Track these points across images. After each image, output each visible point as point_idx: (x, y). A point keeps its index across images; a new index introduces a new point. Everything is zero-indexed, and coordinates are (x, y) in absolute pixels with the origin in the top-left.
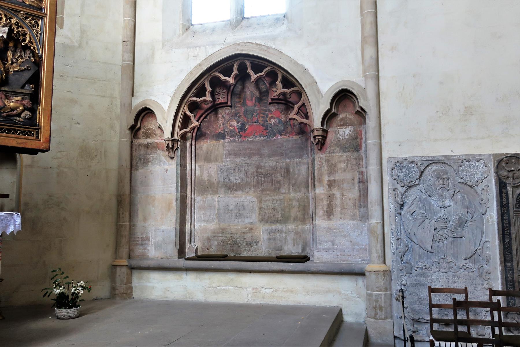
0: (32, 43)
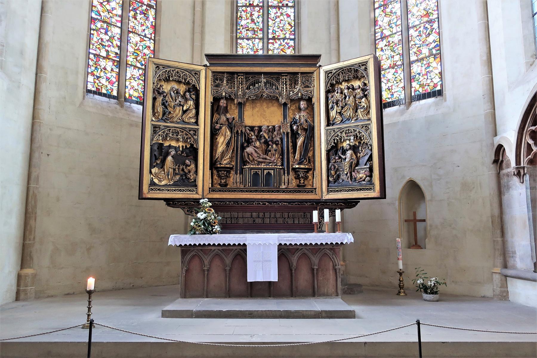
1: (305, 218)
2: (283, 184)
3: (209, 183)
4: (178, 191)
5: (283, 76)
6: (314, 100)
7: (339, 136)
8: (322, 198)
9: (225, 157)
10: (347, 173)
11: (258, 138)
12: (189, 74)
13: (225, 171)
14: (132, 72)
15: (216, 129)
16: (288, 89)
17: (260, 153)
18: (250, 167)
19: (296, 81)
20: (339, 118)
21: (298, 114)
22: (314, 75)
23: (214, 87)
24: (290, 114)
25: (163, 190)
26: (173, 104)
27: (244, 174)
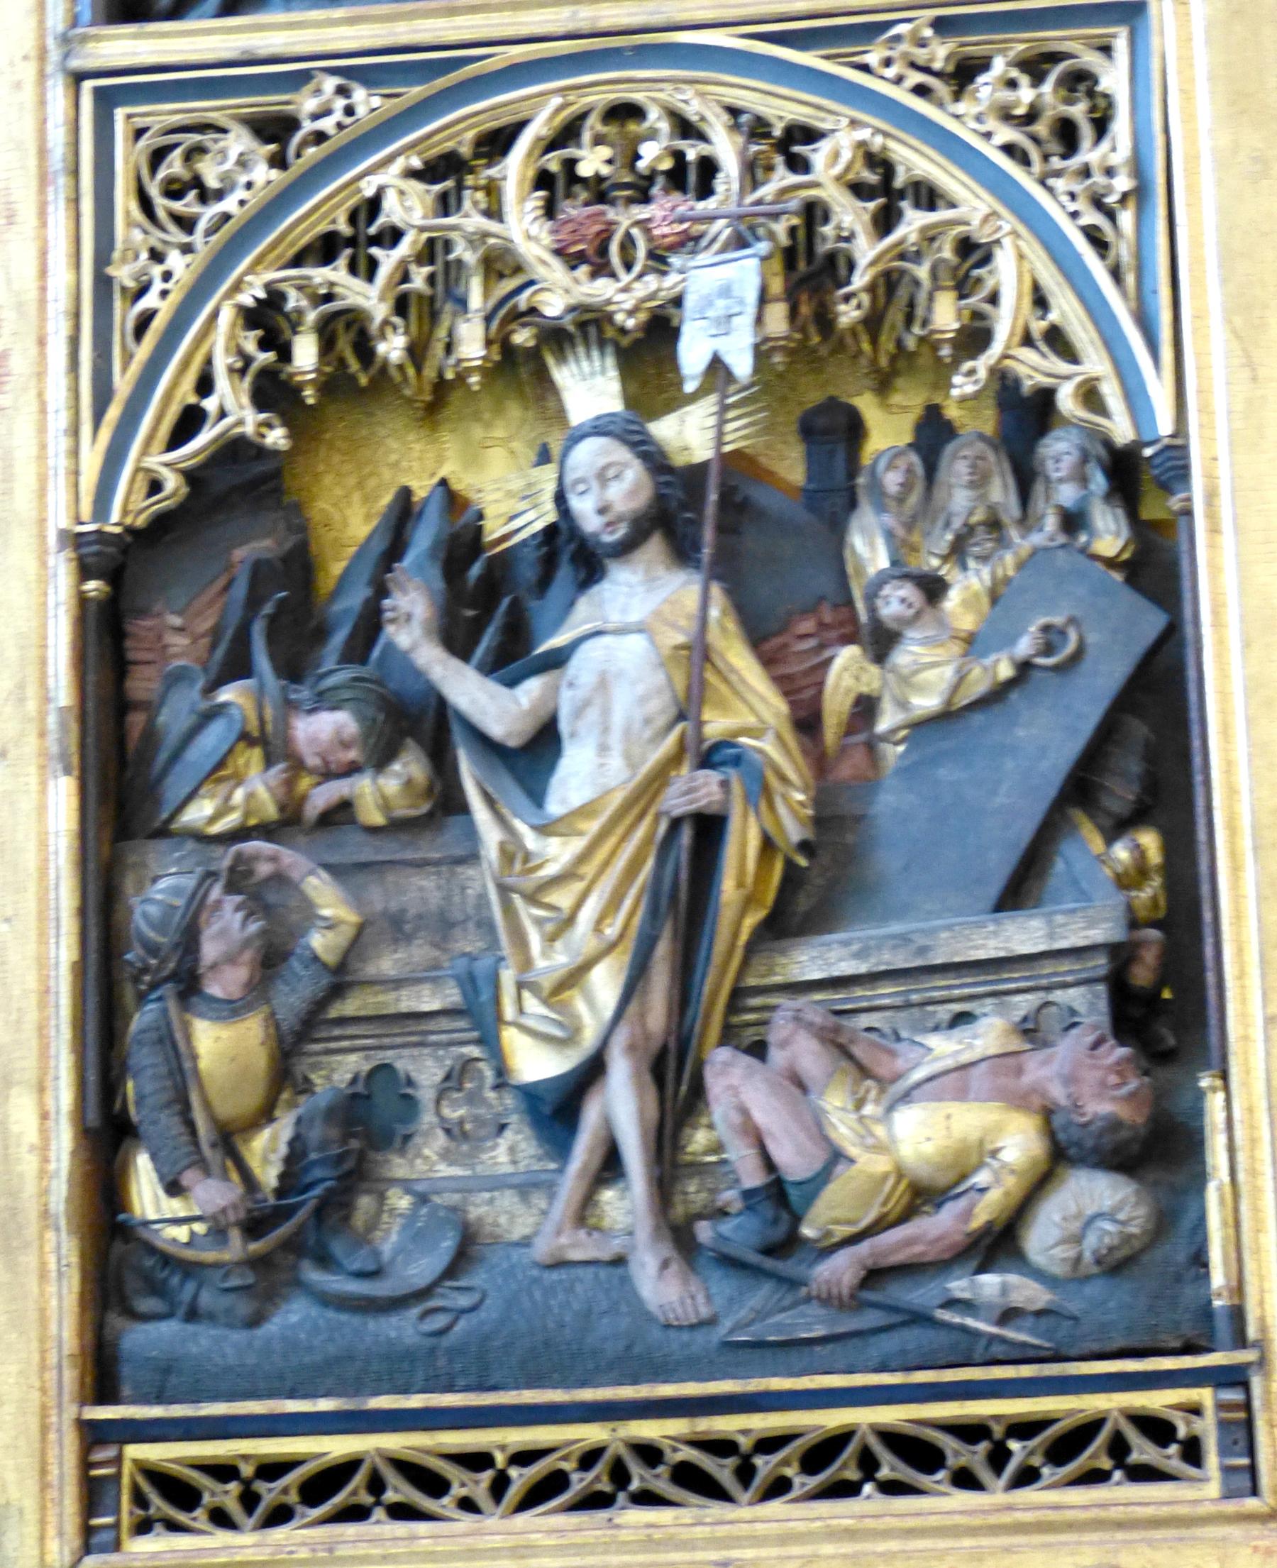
0: (1057, 340)
7: (393, 236)
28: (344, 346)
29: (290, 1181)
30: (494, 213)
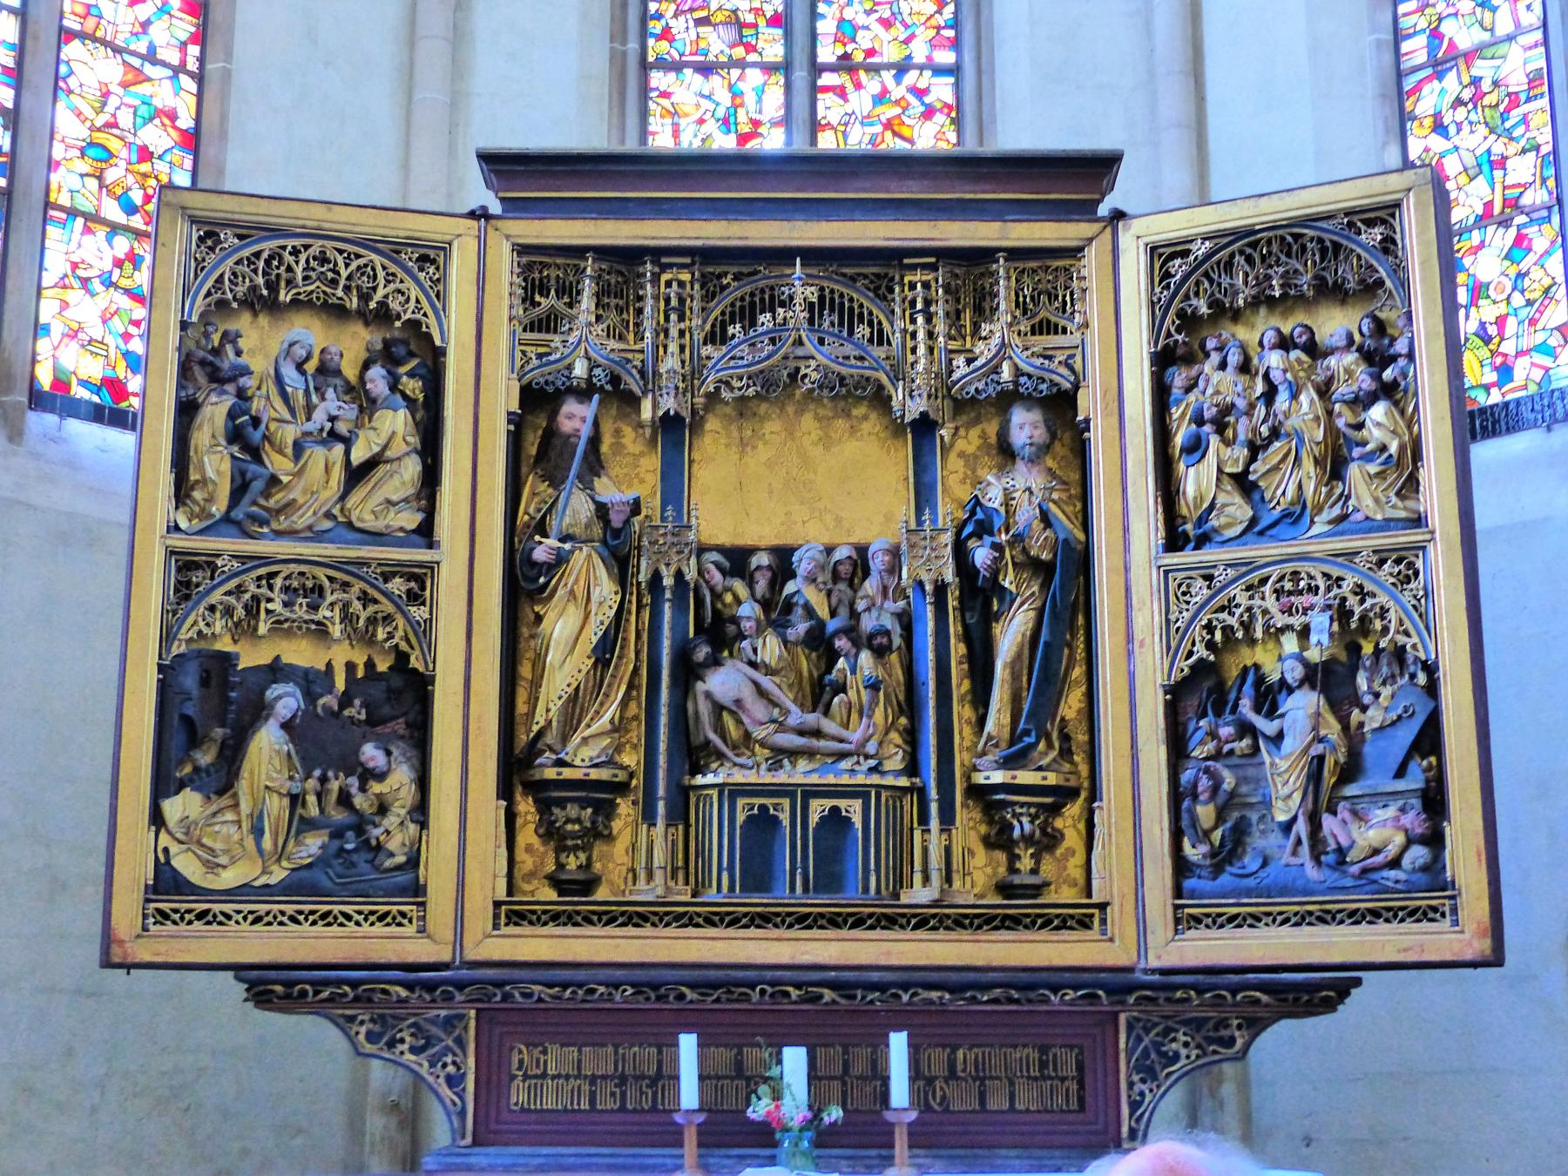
0: (1407, 634)
1: (1051, 1078)
2: (918, 878)
3: (495, 876)
4: (314, 923)
5: (914, 267)
6: (1089, 403)
8: (1143, 960)
9: (589, 726)
10: (1294, 819)
11: (774, 616)
12: (386, 262)
13: (583, 803)
14: (73, 246)
15: (534, 564)
16: (941, 339)
17: (787, 700)
18: (730, 781)
19: (983, 298)
20: (1237, 510)
21: (999, 478)
22: (1084, 262)
23: (525, 330)
24: (953, 480)
25: (229, 917)
26: (289, 433)
27: (692, 820)
28: (1228, 631)
29: (1222, 844)
30: (1263, 599)
